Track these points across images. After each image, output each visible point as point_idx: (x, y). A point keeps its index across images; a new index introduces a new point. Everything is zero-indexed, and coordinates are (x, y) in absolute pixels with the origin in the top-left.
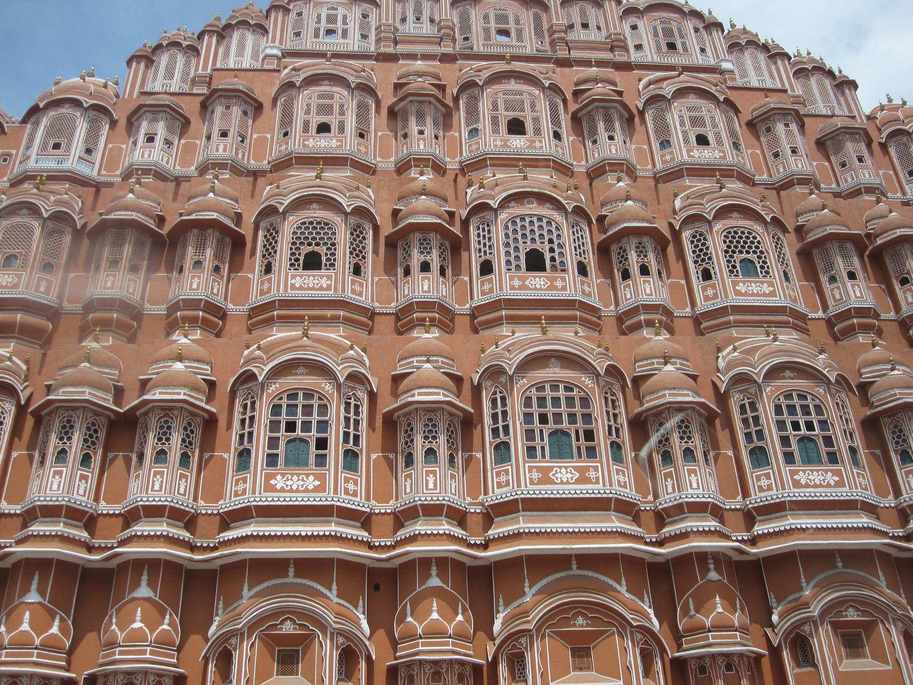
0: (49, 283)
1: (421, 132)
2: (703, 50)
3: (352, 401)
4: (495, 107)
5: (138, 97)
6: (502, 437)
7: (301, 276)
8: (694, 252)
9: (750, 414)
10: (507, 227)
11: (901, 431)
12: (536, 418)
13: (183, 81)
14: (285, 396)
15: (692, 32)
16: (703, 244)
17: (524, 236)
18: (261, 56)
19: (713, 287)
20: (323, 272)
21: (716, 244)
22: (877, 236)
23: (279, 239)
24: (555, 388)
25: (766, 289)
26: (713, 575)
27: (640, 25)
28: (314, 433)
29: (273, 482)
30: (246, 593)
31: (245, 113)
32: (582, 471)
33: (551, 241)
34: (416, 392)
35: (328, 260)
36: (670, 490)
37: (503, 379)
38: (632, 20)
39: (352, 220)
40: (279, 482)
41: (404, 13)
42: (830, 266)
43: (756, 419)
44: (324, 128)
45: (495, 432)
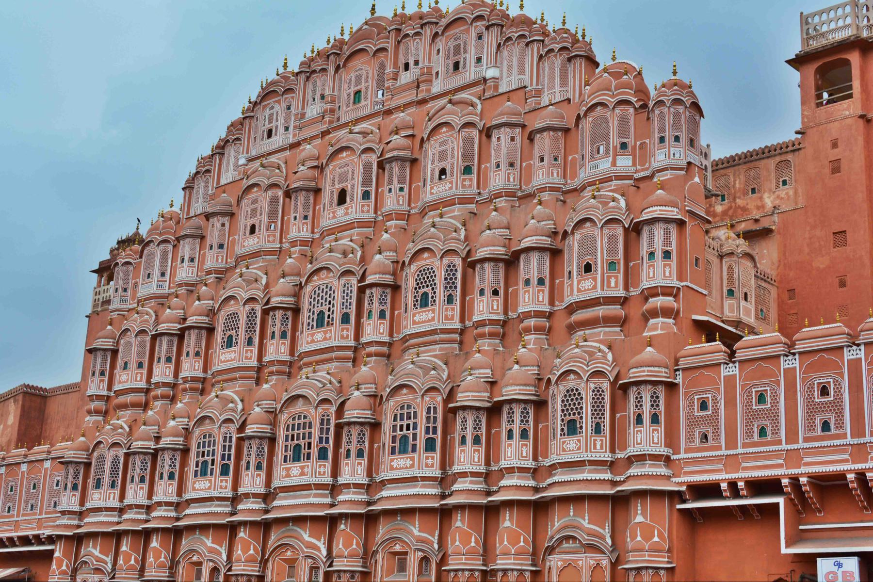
0: (141, 374)
1: (295, 218)
2: (479, 60)
3: (228, 435)
4: (333, 185)
13: (204, 202)
20: (233, 349)
21: (411, 284)
25: (430, 315)
30: (184, 542)
31: (223, 225)
32: (302, 468)
33: (330, 302)
39: (248, 308)
40: (197, 486)
44: (253, 230)
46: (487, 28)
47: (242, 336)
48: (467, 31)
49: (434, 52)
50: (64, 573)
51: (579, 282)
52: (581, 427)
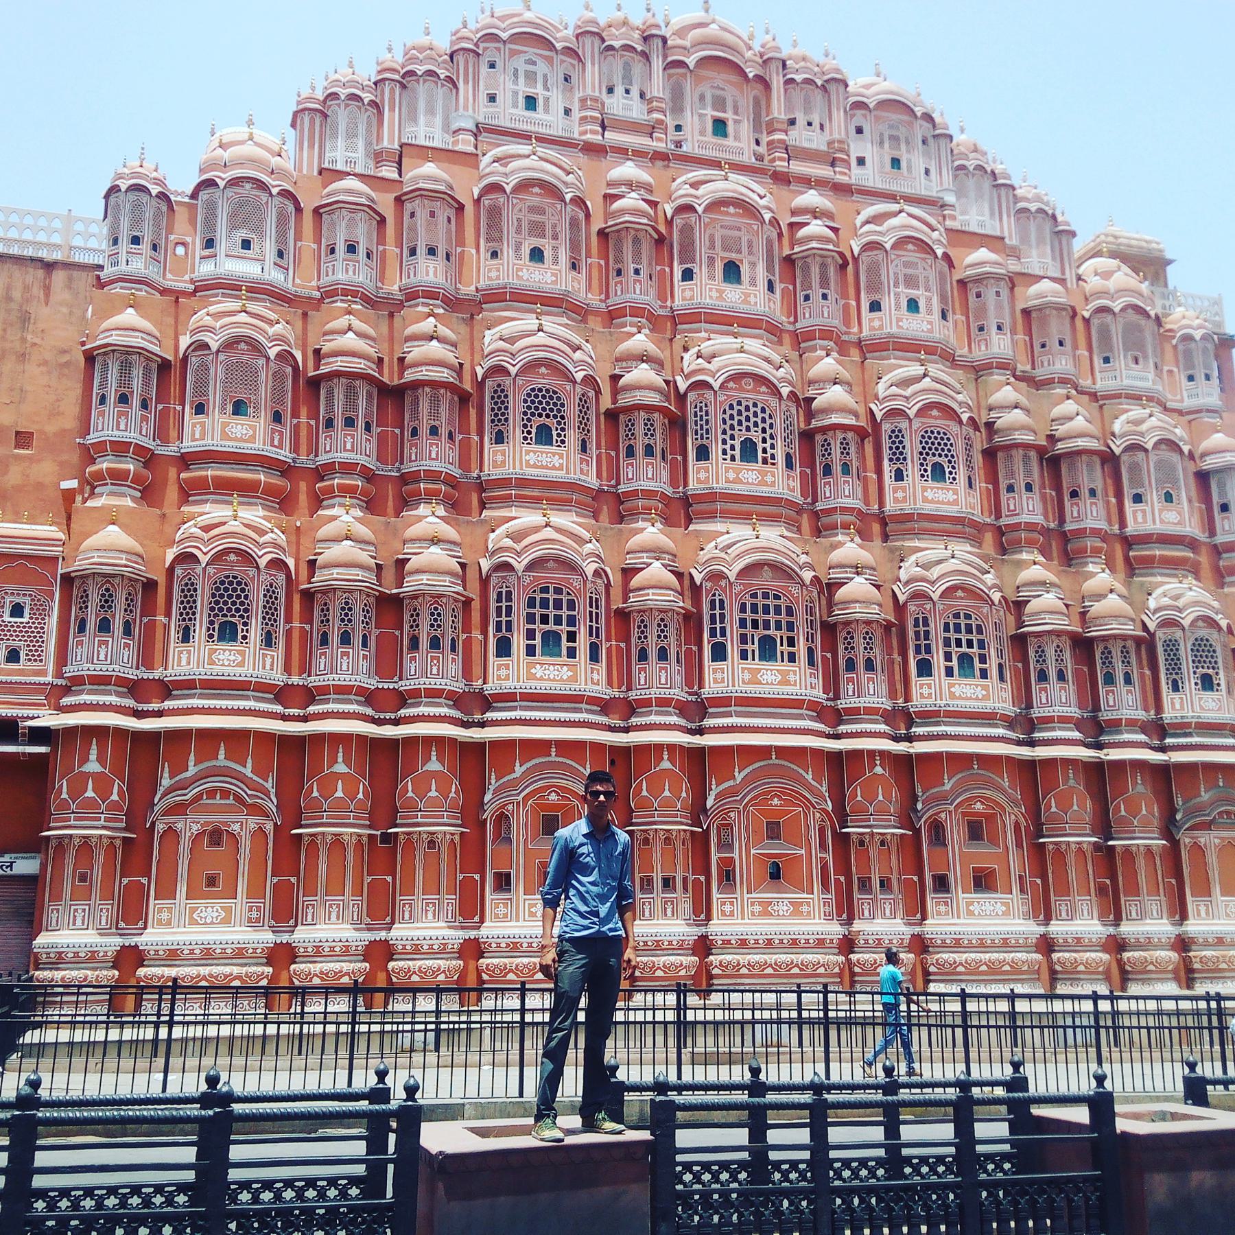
1: (637, 272)
2: (927, 172)
4: (712, 247)
5: (320, 173)
6: (719, 639)
7: (535, 452)
8: (891, 448)
9: (922, 628)
10: (724, 412)
11: (1043, 651)
12: (749, 624)
13: (367, 155)
14: (538, 591)
15: (920, 142)
16: (901, 442)
17: (740, 423)
18: (455, 126)
19: (904, 489)
22: (1060, 440)
23: (511, 405)
24: (765, 596)
25: (951, 496)
26: (878, 770)
27: (866, 129)
28: (563, 628)
29: (533, 671)
30: (519, 770)
32: (784, 674)
33: (764, 431)
34: (650, 591)
35: (559, 435)
36: (850, 693)
37: (723, 583)
38: (859, 118)
40: (538, 671)
41: (610, 80)
42: (1011, 474)
43: (927, 633)
45: (713, 633)
46: (934, 136)
47: (572, 437)
48: (910, 124)
49: (853, 131)
50: (114, 806)
51: (1161, 511)
52: (1219, 685)
